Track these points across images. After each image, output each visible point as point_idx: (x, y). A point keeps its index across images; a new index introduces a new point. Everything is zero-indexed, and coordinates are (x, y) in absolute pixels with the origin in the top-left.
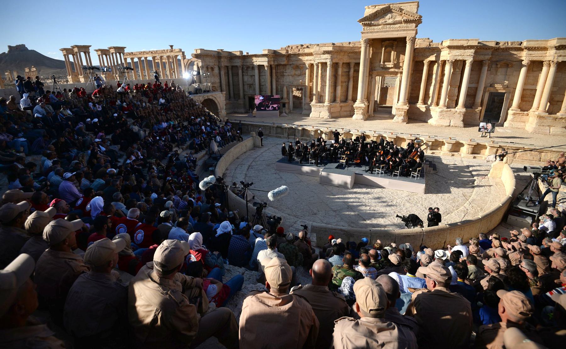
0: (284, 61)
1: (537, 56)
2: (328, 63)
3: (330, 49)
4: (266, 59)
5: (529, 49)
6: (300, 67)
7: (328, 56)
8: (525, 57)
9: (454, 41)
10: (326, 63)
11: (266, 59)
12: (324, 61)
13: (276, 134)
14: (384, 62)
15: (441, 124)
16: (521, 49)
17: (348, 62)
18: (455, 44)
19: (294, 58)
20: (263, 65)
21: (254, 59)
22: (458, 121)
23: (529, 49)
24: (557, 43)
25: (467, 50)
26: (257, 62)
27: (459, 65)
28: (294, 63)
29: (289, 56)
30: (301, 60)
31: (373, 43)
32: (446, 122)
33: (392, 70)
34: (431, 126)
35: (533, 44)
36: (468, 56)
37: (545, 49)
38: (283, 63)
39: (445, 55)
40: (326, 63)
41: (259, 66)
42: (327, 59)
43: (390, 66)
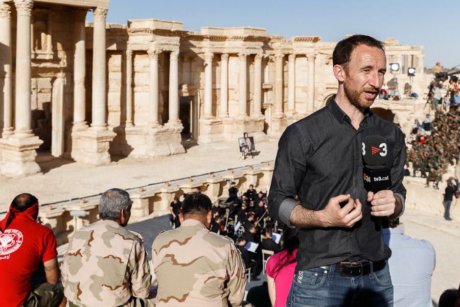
1: (218, 46)
5: (212, 38)
8: (206, 50)
9: (158, 23)
15: (162, 153)
16: (200, 38)
23: (212, 38)
24: (245, 33)
25: (172, 38)
27: (164, 58)
32: (164, 149)
33: (49, 65)
35: (214, 33)
36: (173, 45)
37: (223, 39)
39: (134, 42)
43: (47, 57)
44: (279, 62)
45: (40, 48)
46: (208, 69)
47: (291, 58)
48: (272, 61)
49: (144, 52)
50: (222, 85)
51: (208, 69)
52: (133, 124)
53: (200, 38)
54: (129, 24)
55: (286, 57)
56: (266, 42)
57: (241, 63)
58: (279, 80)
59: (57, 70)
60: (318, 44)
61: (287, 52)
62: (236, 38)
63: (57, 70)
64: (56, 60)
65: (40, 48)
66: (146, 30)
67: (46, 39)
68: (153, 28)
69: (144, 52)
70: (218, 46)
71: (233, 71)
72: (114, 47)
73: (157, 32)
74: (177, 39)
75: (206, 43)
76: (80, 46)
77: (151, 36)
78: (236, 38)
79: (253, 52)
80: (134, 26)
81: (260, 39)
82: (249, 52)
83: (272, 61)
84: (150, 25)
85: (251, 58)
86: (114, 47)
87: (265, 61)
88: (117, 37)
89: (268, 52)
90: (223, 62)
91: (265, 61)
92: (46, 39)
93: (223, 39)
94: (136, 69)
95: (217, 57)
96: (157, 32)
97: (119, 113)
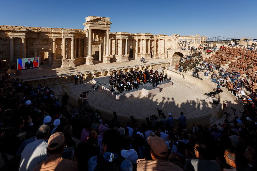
0: (35, 36)
1: (139, 37)
2: (72, 39)
3: (74, 32)
4: (24, 34)
5: (138, 36)
6: (49, 41)
7: (73, 35)
8: (136, 38)
10: (70, 39)
11: (24, 34)
12: (70, 37)
13: (60, 82)
14: (94, 39)
16: (135, 36)
17: (78, 38)
18: (123, 33)
19: (42, 35)
20: (21, 38)
21: (9, 33)
22: (127, 60)
23: (138, 36)
26: (11, 36)
27: (124, 41)
28: (42, 37)
29: (39, 33)
30: (47, 36)
31: (93, 31)
34: (118, 63)
35: (138, 35)
36: (126, 38)
37: (141, 36)
38: (35, 37)
39: (117, 37)
40: (70, 39)
41: (15, 39)
42: (72, 37)
43: (97, 41)
44: (155, 41)
45: (96, 39)
46: (137, 42)
47: (159, 40)
48: (154, 41)
49: (119, 39)
50: (141, 46)
51: (137, 42)
52: (117, 55)
53: (135, 36)
54: (116, 33)
55: (157, 40)
56: (152, 37)
57: (144, 42)
58: (155, 45)
59: (100, 43)
60: (166, 37)
61: (157, 39)
62: (143, 36)
63: (100, 43)
64: (99, 41)
65: (96, 39)
66: (119, 34)
67: (97, 36)
68: (121, 34)
69: (119, 39)
70: (139, 37)
71: (143, 43)
72: (113, 38)
73: (122, 35)
74: (127, 36)
75: (136, 37)
76: (105, 37)
77: (121, 36)
78: (143, 36)
79: (148, 39)
80: (117, 33)
81: (150, 36)
82: (147, 39)
83: (154, 41)
84: (120, 33)
85: (147, 40)
86: (113, 38)
87: (151, 41)
88: (113, 36)
89: (153, 39)
90: (141, 41)
91: (151, 41)
92: (97, 36)
93: (141, 36)
94: (118, 43)
95: (139, 40)
96: (122, 35)
97: (114, 52)
